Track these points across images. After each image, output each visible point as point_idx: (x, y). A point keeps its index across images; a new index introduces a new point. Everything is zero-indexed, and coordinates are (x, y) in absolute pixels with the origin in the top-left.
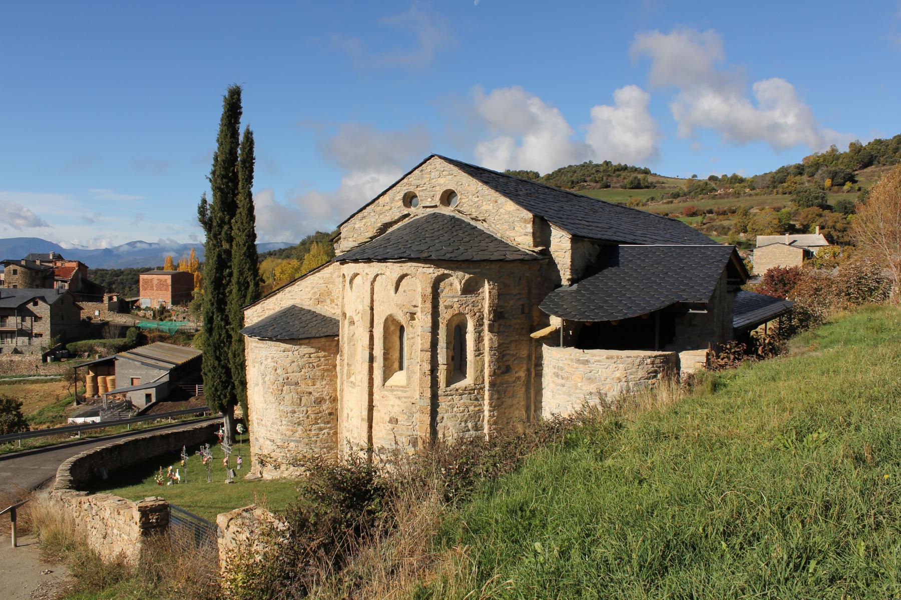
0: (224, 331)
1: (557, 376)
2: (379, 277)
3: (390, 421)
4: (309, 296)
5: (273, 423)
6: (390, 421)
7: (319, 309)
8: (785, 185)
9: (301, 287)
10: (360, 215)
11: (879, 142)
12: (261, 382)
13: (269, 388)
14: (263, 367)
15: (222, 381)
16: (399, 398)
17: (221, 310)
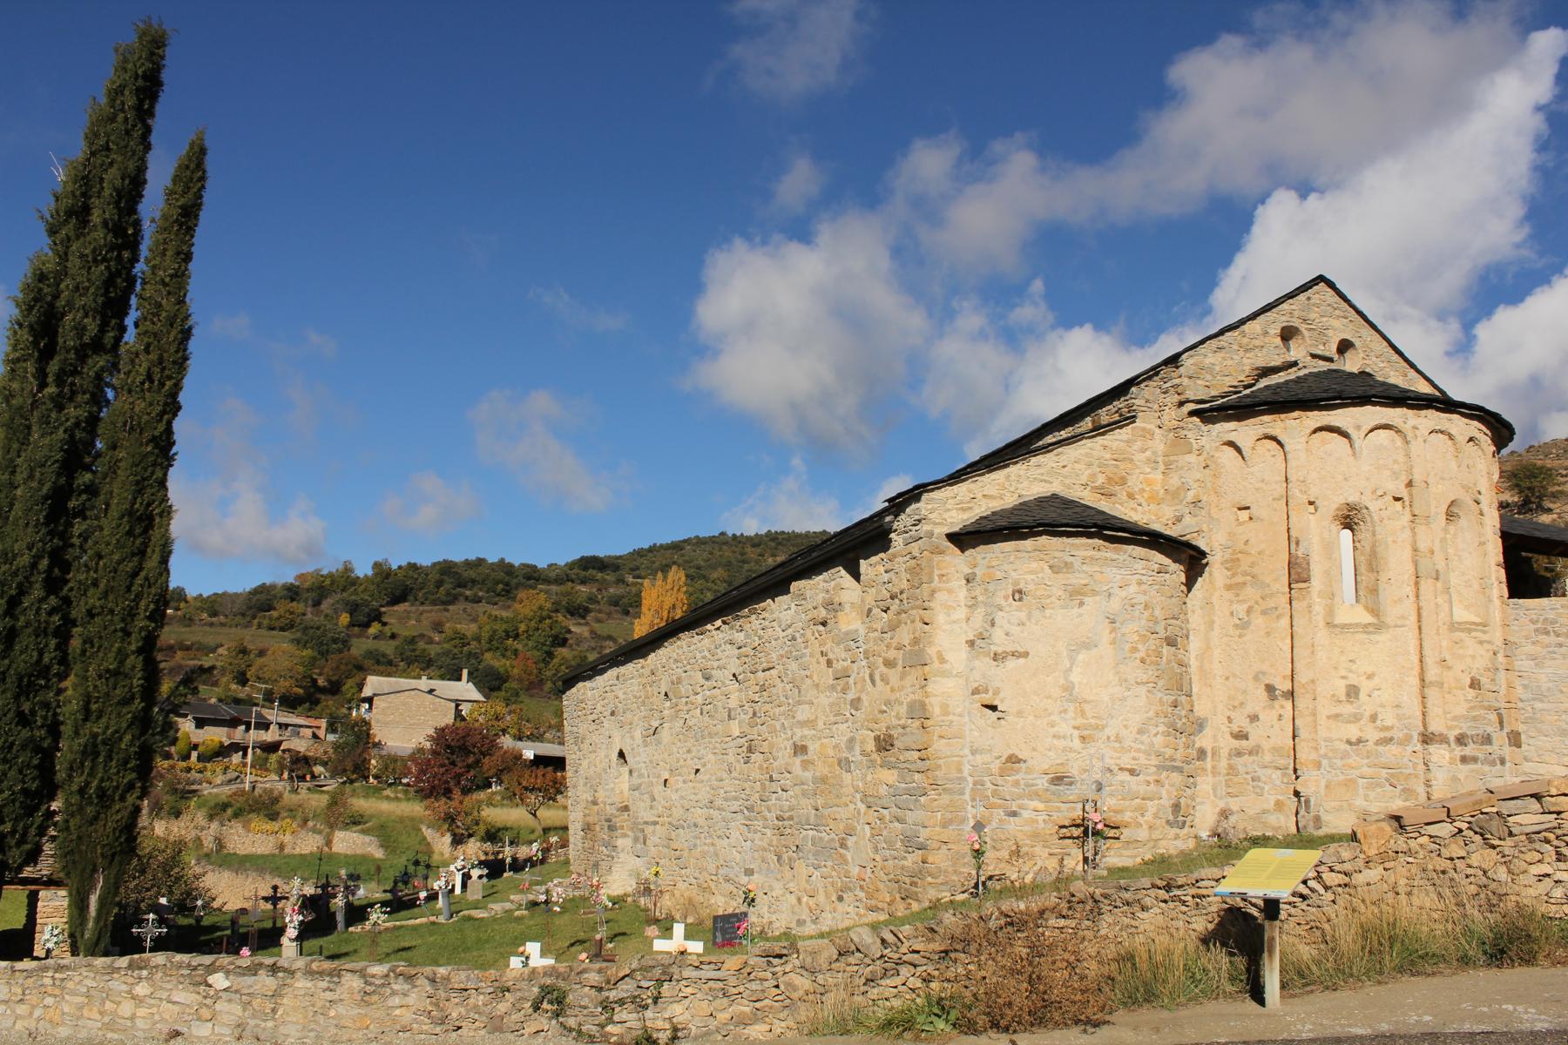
0: (53, 642)
1: (1547, 633)
2: (1399, 441)
3: (1472, 686)
4: (1084, 479)
5: (1140, 732)
6: (1472, 686)
7: (1104, 506)
8: (275, 614)
9: (1063, 460)
10: (1214, 343)
11: (413, 567)
12: (1105, 637)
13: (1135, 650)
14: (1115, 605)
15: (25, 791)
16: (1481, 643)
17: (53, 585)
